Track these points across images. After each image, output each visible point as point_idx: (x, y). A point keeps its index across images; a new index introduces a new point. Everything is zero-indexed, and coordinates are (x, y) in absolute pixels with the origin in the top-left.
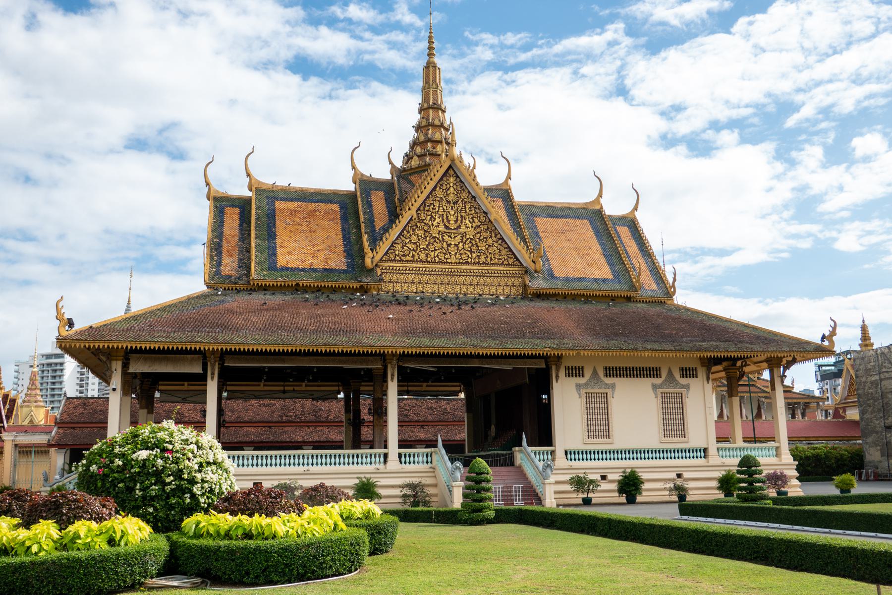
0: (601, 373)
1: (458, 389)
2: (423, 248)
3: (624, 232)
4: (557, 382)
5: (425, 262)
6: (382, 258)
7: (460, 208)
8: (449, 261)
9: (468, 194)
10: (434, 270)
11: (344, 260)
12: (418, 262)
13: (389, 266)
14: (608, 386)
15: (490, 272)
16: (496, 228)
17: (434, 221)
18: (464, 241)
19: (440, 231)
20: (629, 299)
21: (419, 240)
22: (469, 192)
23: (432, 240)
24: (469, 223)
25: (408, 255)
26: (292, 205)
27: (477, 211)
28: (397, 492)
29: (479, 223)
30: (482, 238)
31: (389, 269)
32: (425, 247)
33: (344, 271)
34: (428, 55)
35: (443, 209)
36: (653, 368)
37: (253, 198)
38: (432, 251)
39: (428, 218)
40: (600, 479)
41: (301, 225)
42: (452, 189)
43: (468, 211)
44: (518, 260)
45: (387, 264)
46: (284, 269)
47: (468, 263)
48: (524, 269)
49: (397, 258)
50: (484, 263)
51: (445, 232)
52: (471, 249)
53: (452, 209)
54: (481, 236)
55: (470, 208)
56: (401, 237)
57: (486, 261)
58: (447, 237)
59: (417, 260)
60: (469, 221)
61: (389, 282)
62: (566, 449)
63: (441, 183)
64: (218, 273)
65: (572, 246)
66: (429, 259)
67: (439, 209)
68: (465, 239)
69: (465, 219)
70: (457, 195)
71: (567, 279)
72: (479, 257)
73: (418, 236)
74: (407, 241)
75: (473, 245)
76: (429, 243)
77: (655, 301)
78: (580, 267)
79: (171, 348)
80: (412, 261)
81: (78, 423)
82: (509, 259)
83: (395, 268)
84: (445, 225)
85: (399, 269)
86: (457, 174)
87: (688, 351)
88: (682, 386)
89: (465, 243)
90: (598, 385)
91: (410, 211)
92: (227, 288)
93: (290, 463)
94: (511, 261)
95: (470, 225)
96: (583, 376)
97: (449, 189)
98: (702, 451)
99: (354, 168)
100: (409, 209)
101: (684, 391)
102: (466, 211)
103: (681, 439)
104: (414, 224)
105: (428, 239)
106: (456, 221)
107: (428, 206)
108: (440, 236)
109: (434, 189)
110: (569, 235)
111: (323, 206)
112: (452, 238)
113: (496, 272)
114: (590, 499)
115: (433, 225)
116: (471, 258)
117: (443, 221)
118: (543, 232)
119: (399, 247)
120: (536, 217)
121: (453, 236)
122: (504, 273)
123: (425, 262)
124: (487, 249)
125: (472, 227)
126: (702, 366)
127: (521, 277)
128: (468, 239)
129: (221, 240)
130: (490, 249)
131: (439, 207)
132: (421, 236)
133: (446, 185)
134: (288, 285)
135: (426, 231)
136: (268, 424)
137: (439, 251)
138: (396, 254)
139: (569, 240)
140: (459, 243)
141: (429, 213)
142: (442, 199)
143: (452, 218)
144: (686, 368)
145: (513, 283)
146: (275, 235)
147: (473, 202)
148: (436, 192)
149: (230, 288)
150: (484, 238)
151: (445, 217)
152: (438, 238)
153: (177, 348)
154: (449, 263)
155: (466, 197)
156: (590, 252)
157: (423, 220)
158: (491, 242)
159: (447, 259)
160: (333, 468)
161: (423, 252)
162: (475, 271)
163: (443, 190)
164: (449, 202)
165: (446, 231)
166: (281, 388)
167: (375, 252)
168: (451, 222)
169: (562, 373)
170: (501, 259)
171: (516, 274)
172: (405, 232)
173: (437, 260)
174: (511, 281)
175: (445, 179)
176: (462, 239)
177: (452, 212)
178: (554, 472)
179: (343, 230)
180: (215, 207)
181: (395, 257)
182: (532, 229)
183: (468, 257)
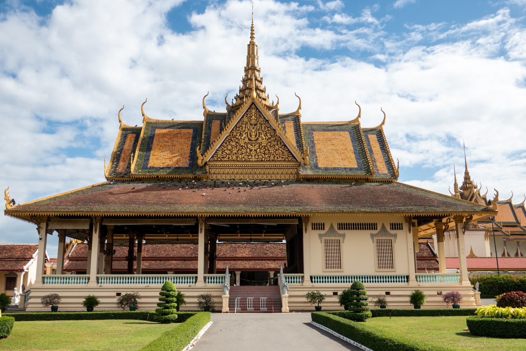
0: (336, 227)
1: (282, 237)
2: (235, 153)
3: (373, 138)
4: (306, 232)
5: (236, 161)
6: (210, 160)
7: (258, 128)
8: (251, 160)
9: (263, 119)
10: (241, 166)
11: (188, 162)
12: (231, 161)
13: (214, 164)
14: (340, 235)
15: (276, 166)
16: (281, 139)
17: (242, 136)
18: (260, 147)
19: (245, 142)
20: (367, 180)
21: (233, 148)
22: (264, 118)
23: (241, 148)
24: (263, 136)
25: (226, 157)
26: (164, 131)
28: (196, 300)
29: (270, 137)
30: (272, 145)
31: (214, 166)
32: (236, 152)
33: (187, 168)
34: (251, 38)
35: (248, 129)
36: (372, 224)
39: (238, 135)
40: (385, 294)
41: (168, 142)
42: (253, 116)
43: (263, 129)
44: (294, 158)
45: (213, 163)
47: (263, 161)
48: (298, 164)
49: (219, 159)
50: (273, 161)
52: (265, 152)
53: (253, 129)
54: (271, 144)
55: (265, 127)
56: (222, 146)
57: (274, 159)
58: (250, 145)
59: (231, 160)
60: (264, 135)
61: (214, 174)
62: (311, 275)
63: (246, 113)
64: (114, 172)
65: (334, 148)
66: (238, 159)
67: (245, 129)
68: (261, 146)
69: (261, 134)
70: (256, 120)
71: (326, 169)
72: (269, 157)
73: (232, 146)
75: (266, 150)
76: (239, 150)
77: (385, 181)
78: (336, 161)
79: (66, 215)
80: (228, 161)
81: (79, 258)
82: (289, 158)
84: (249, 138)
85: (220, 166)
86: (257, 107)
87: (389, 212)
88: (392, 235)
89: (261, 149)
90: (333, 234)
92: (118, 180)
93: (208, 281)
95: (265, 138)
96: (324, 229)
97: (251, 117)
98: (405, 277)
100: (226, 130)
101: (393, 239)
102: (262, 129)
104: (230, 138)
105: (238, 147)
106: (256, 136)
107: (238, 127)
108: (246, 145)
109: (243, 117)
110: (334, 142)
111: (184, 131)
113: (280, 166)
114: (321, 307)
115: (241, 139)
116: (265, 158)
117: (248, 136)
119: (220, 152)
121: (253, 145)
122: (286, 166)
123: (236, 161)
124: (275, 152)
125: (266, 139)
126: (406, 222)
127: (297, 168)
128: (263, 146)
129: (121, 153)
131: (245, 128)
132: (234, 146)
133: (250, 114)
134: (152, 177)
135: (237, 143)
137: (245, 154)
138: (218, 157)
139: (333, 145)
140: (257, 149)
141: (239, 132)
142: (248, 123)
143: (253, 134)
144: (397, 224)
145: (291, 172)
146: (151, 148)
147: (267, 123)
148: (244, 119)
149: (120, 180)
150: (273, 145)
152: (244, 147)
153: (70, 215)
154: (251, 161)
155: (262, 121)
156: (345, 151)
157: (235, 136)
158: (278, 147)
159: (249, 159)
160: (62, 285)
162: (267, 165)
163: (248, 117)
166: (176, 238)
167: (204, 156)
168: (252, 137)
169: (309, 227)
170: (284, 158)
171: (293, 166)
172: (224, 144)
173: (243, 159)
174: (289, 171)
176: (259, 147)
177: (253, 131)
179: (192, 144)
180: (122, 134)
181: (218, 159)
183: (263, 157)
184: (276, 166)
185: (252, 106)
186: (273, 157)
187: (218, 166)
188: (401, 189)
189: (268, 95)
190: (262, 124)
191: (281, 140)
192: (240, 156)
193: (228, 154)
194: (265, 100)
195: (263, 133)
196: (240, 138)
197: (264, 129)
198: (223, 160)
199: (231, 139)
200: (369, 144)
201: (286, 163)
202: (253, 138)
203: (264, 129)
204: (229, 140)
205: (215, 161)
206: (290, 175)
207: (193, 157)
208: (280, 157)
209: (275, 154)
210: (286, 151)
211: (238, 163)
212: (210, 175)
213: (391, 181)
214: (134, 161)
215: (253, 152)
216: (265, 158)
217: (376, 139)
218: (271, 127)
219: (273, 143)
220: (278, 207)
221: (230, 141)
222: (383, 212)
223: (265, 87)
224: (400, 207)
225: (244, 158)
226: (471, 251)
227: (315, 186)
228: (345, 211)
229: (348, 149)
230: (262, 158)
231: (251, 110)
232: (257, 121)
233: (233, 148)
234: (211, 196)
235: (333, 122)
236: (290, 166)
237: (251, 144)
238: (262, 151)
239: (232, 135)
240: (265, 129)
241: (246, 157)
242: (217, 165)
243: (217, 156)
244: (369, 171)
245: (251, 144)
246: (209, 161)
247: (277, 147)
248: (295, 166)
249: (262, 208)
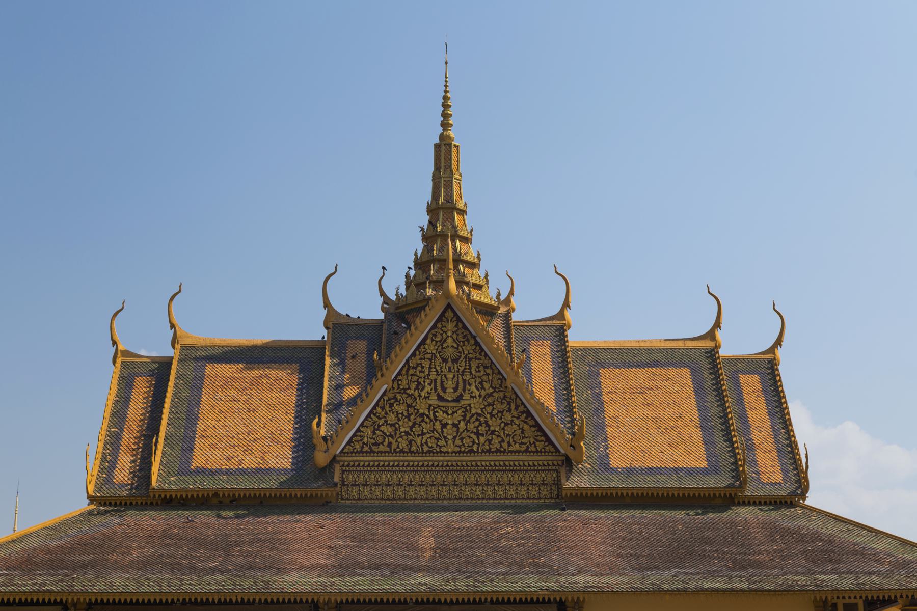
3: (751, 383)
5: (407, 453)
7: (461, 369)
9: (474, 347)
10: (421, 464)
11: (289, 454)
15: (507, 463)
16: (517, 396)
17: (421, 391)
18: (467, 418)
19: (430, 405)
21: (399, 420)
22: (477, 344)
23: (419, 419)
24: (475, 390)
25: (382, 443)
27: (489, 371)
29: (491, 390)
30: (495, 412)
31: (353, 466)
32: (408, 429)
35: (437, 371)
37: (175, 362)
38: (418, 435)
39: (414, 386)
42: (450, 340)
43: (474, 372)
45: (350, 458)
46: (201, 471)
47: (474, 452)
48: (560, 458)
49: (366, 449)
50: (498, 451)
51: (439, 406)
52: (478, 430)
53: (450, 370)
54: (493, 409)
55: (478, 367)
56: (372, 416)
57: (501, 447)
59: (395, 450)
60: (476, 387)
61: (353, 485)
63: (433, 332)
65: (652, 414)
66: (414, 448)
67: (430, 371)
69: (470, 385)
70: (457, 348)
72: (490, 441)
73: (398, 414)
74: (381, 422)
75: (480, 424)
76: (414, 424)
78: (655, 450)
82: (537, 443)
84: (438, 395)
85: (369, 466)
87: (770, 591)
89: (469, 421)
91: (384, 379)
94: (540, 446)
95: (478, 393)
97: (445, 341)
99: (327, 304)
104: (392, 396)
105: (412, 417)
106: (456, 389)
107: (413, 368)
109: (423, 342)
112: (448, 415)
113: (516, 463)
115: (420, 396)
116: (478, 444)
117: (436, 390)
118: (610, 392)
120: (604, 368)
121: (450, 412)
122: (529, 465)
123: (407, 453)
124: (503, 429)
125: (480, 396)
127: (557, 470)
128: (473, 415)
129: (122, 430)
130: (509, 430)
131: (430, 368)
132: (402, 414)
133: (442, 334)
135: (409, 406)
137: (428, 436)
138: (364, 443)
139: (648, 405)
140: (459, 421)
141: (415, 378)
142: (435, 357)
143: (450, 385)
145: (543, 481)
146: (197, 418)
147: (483, 358)
148: (426, 347)
150: (499, 412)
154: (445, 453)
155: (471, 351)
156: (679, 423)
157: (405, 390)
158: (510, 417)
159: (441, 447)
161: (405, 437)
162: (483, 463)
163: (437, 342)
164: (445, 360)
167: (329, 443)
168: (448, 391)
171: (549, 465)
172: (379, 410)
173: (426, 448)
175: (439, 325)
176: (465, 416)
177: (450, 376)
180: (122, 378)
181: (363, 447)
182: (592, 388)
183: (474, 442)
184: (505, 465)
185: (446, 315)
186: (500, 443)
187: (363, 466)
188: (812, 524)
189: (487, 275)
190: (470, 359)
191: (518, 399)
192: (418, 440)
193: (388, 436)
194: (478, 287)
195: (473, 381)
196: (416, 394)
197: (477, 372)
198: (376, 450)
199: (395, 398)
200: (740, 400)
201: (530, 458)
202: (449, 395)
203: (477, 372)
204: (389, 400)
205: (355, 453)
206: (542, 488)
208: (515, 442)
209: (502, 435)
210: (531, 426)
211: (411, 458)
212: (344, 489)
213: (791, 502)
214: (157, 452)
215: (449, 432)
216: (478, 444)
217: (759, 386)
218: (493, 366)
219: (499, 406)
220: (509, 578)
221: (392, 401)
222: (756, 591)
223: (479, 254)
224: (797, 578)
225: (427, 445)
227: (602, 514)
228: (665, 587)
229: (687, 418)
230: (471, 444)
231: (444, 324)
232: (460, 352)
233: (399, 420)
234: (347, 547)
235: (651, 341)
236: (539, 465)
237: (444, 409)
238: (471, 426)
239: (399, 388)
240: (480, 371)
241: (432, 443)
242: (362, 464)
243: (361, 440)
244: (737, 473)
245: (444, 409)
246: (342, 452)
247: (508, 417)
248: (554, 465)
249: (471, 582)
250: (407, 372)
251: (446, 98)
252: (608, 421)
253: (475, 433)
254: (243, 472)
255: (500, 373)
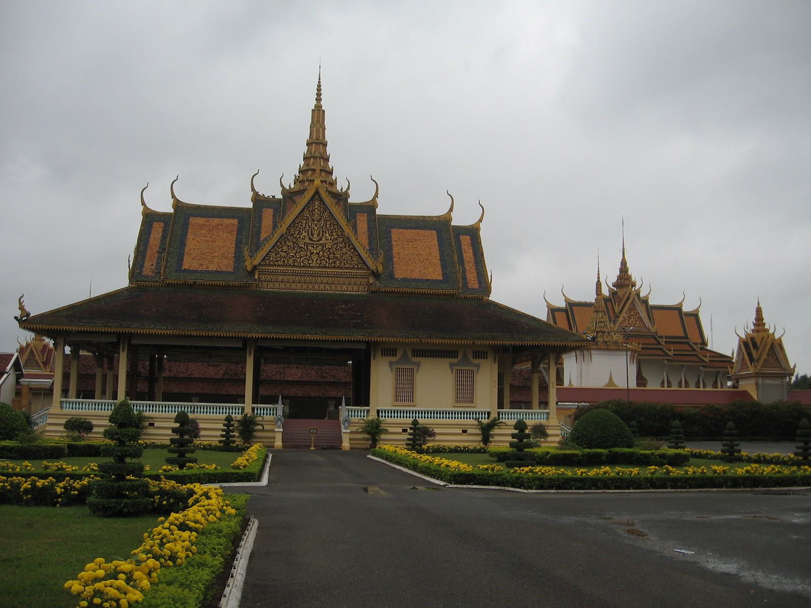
0: (410, 355)
4: (374, 359)
6: (260, 263)
13: (266, 269)
14: (414, 363)
19: (305, 243)
21: (289, 249)
22: (330, 212)
23: (299, 250)
26: (201, 221)
27: (336, 227)
29: (336, 237)
31: (265, 271)
38: (299, 258)
43: (328, 227)
47: (327, 267)
49: (271, 263)
50: (339, 267)
52: (329, 256)
53: (316, 226)
55: (330, 224)
57: (340, 265)
67: (306, 226)
68: (325, 249)
69: (326, 233)
71: (405, 280)
75: (330, 253)
83: (269, 271)
84: (310, 238)
89: (324, 252)
95: (330, 238)
96: (396, 356)
97: (314, 210)
99: (253, 189)
102: (326, 227)
103: (470, 405)
106: (318, 235)
107: (297, 223)
111: (226, 221)
115: (300, 238)
122: (354, 275)
125: (331, 239)
131: (306, 224)
132: (291, 246)
135: (294, 243)
136: (212, 381)
137: (304, 258)
140: (320, 252)
141: (298, 229)
142: (309, 218)
146: (185, 245)
150: (340, 248)
151: (310, 232)
157: (293, 234)
159: (310, 264)
163: (310, 211)
165: (310, 242)
167: (253, 259)
169: (379, 354)
175: (311, 202)
177: (316, 228)
178: (351, 425)
183: (327, 262)
185: (315, 197)
189: (336, 179)
190: (326, 220)
193: (283, 257)
202: (315, 238)
204: (284, 239)
207: (238, 257)
212: (260, 283)
215: (315, 257)
226: (611, 378)
238: (325, 254)
242: (269, 271)
247: (344, 250)
250: (294, 225)
251: (319, 86)
252: (394, 255)
253: (327, 258)
254: (208, 272)
255: (341, 228)
